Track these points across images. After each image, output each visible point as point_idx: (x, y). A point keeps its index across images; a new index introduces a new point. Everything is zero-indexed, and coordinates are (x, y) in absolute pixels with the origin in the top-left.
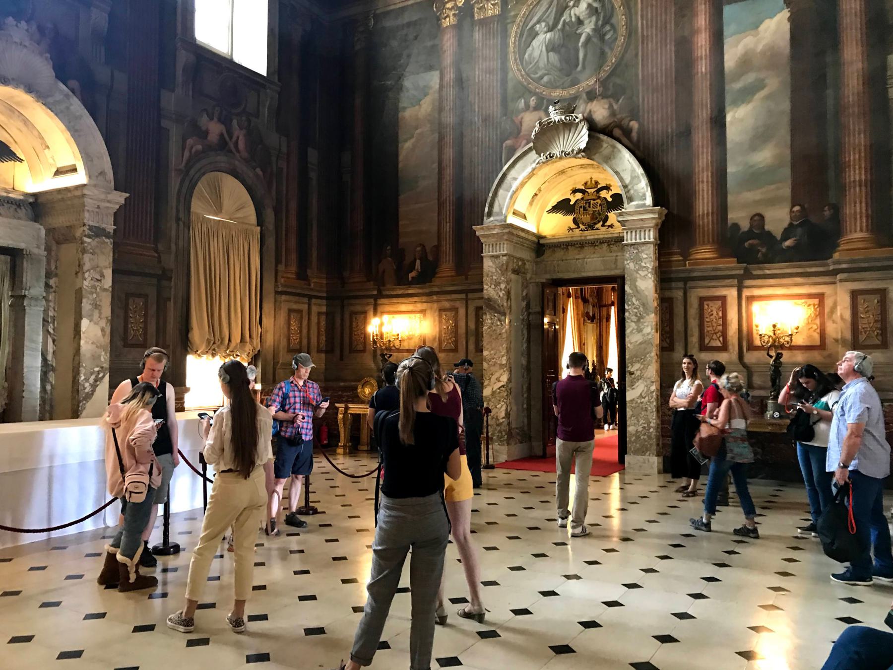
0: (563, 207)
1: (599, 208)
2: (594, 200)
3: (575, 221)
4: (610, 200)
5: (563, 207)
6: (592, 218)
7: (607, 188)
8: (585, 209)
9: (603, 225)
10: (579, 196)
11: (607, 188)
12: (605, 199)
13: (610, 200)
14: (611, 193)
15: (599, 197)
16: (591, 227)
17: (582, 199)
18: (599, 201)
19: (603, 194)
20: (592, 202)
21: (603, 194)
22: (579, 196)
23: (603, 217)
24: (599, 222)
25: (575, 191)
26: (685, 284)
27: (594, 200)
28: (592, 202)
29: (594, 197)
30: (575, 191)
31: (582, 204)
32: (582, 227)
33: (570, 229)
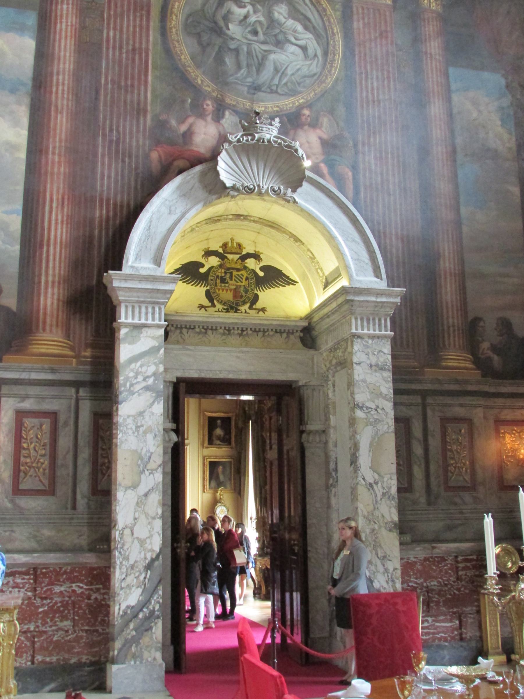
0: (190, 272)
1: (244, 283)
2: (238, 270)
3: (209, 295)
4: (261, 274)
5: (190, 272)
6: (235, 296)
7: (256, 256)
8: (223, 280)
9: (251, 308)
10: (214, 261)
11: (256, 256)
12: (254, 271)
13: (261, 274)
14: (262, 264)
15: (245, 268)
16: (232, 307)
17: (221, 266)
18: (243, 272)
19: (251, 263)
20: (235, 273)
21: (251, 263)
22: (214, 261)
23: (251, 296)
24: (244, 303)
25: (208, 253)
26: (424, 398)
27: (238, 270)
28: (235, 273)
29: (239, 266)
30: (208, 253)
31: (221, 273)
32: (219, 306)
33: (201, 307)
